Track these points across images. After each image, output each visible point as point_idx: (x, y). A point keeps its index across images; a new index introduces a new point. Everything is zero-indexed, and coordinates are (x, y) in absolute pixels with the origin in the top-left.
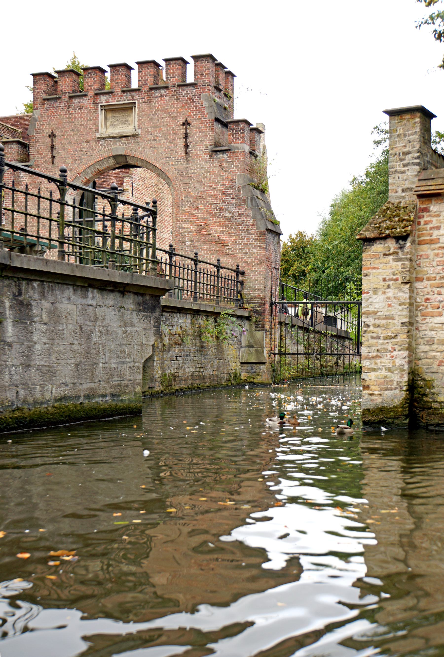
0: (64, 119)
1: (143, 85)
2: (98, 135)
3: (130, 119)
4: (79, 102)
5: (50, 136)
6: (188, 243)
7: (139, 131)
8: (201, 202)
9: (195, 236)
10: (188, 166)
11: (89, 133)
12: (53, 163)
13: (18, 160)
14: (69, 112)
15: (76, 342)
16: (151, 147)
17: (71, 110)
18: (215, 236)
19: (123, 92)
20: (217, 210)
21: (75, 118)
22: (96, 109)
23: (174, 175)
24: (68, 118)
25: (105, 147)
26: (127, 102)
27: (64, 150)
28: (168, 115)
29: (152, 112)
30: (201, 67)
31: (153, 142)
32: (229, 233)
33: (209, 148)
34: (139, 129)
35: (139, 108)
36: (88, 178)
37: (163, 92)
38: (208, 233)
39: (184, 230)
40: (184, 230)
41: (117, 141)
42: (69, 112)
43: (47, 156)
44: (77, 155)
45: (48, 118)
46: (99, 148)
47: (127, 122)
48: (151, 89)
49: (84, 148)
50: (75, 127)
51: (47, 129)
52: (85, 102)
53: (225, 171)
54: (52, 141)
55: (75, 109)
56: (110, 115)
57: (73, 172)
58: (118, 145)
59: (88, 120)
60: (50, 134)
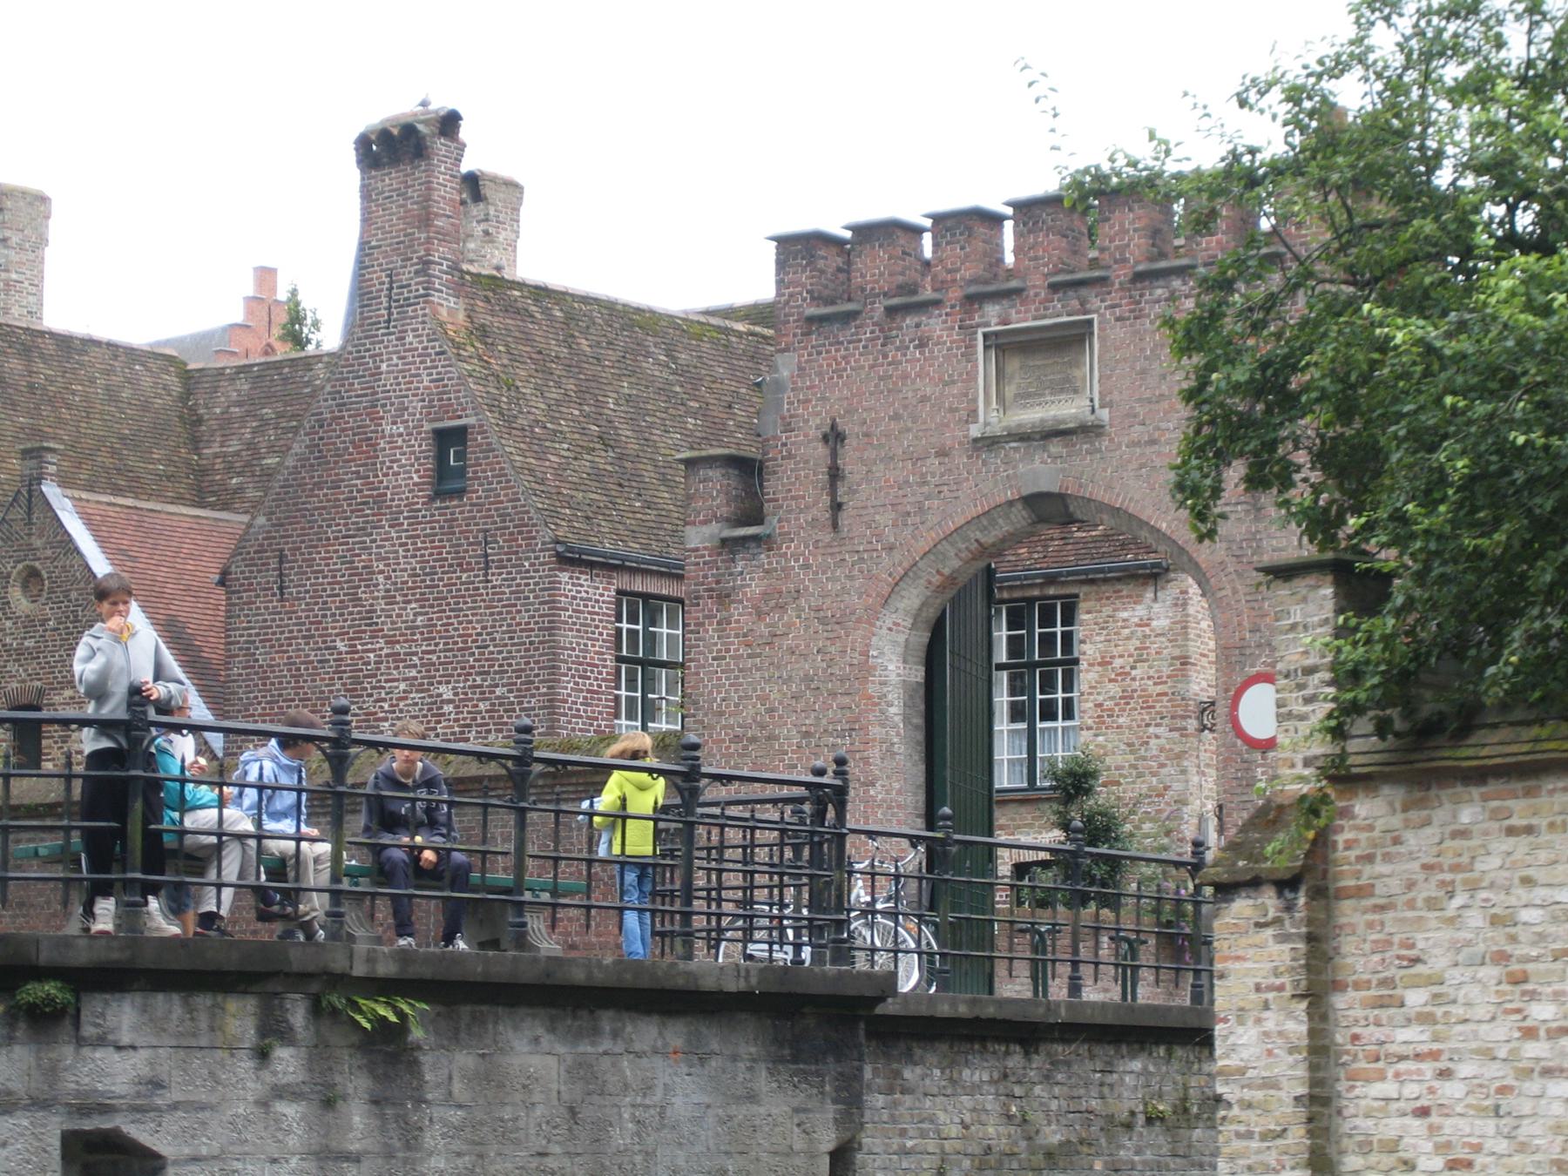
1: (1116, 262)
2: (975, 431)
3: (1077, 373)
4: (918, 326)
5: (825, 438)
7: (1104, 414)
10: (1261, 526)
11: (947, 425)
12: (835, 526)
13: (728, 520)
15: (557, 1149)
17: (891, 352)
19: (1055, 288)
21: (905, 377)
22: (971, 346)
24: (881, 379)
27: (869, 482)
29: (1142, 350)
31: (1148, 450)
34: (1102, 407)
35: (1102, 339)
36: (947, 571)
37: (1176, 283)
42: (885, 356)
43: (816, 503)
44: (911, 499)
45: (821, 380)
46: (979, 472)
47: (1069, 387)
48: (1139, 277)
50: (905, 407)
51: (819, 414)
52: (935, 325)
54: (834, 455)
55: (903, 348)
56: (1013, 364)
57: (897, 556)
58: (1037, 462)
59: (946, 384)
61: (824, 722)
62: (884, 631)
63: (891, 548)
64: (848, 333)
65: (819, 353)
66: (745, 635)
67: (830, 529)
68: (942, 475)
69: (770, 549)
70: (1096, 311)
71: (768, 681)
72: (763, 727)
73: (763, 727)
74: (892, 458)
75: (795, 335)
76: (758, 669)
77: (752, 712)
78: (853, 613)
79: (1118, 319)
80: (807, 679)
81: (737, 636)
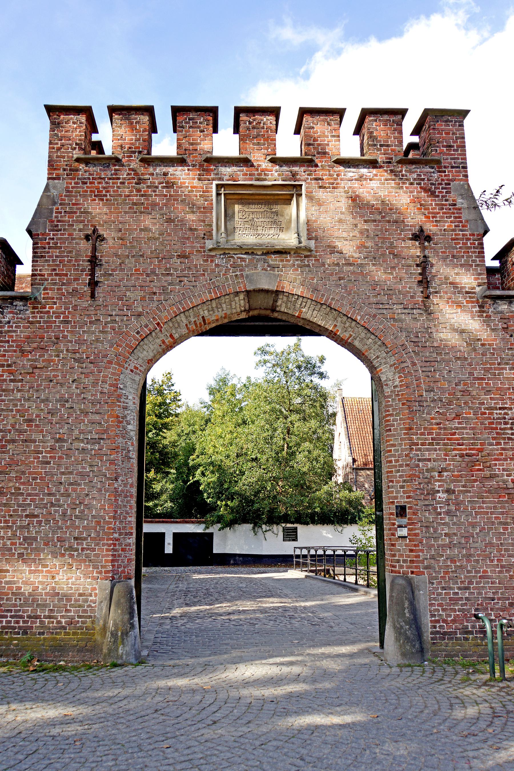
0: (127, 204)
1: (318, 153)
6: (442, 496)
9: (456, 479)
12: (93, 296)
14: (139, 191)
16: (340, 279)
17: (143, 186)
18: (505, 482)
20: (506, 423)
23: (399, 343)
25: (227, 270)
28: (379, 217)
30: (446, 134)
33: (478, 289)
37: (364, 171)
38: (487, 473)
39: (430, 465)
40: (430, 465)
41: (258, 260)
44: (159, 284)
46: (213, 271)
49: (176, 270)
54: (94, 249)
57: (144, 320)
60: (90, 232)
61: (77, 432)
62: (128, 371)
63: (139, 315)
64: (109, 173)
66: (9, 366)
67: (89, 298)
68: (184, 270)
69: (34, 308)
70: (305, 181)
73: (20, 432)
75: (64, 170)
76: (19, 391)
77: (12, 421)
78: (106, 356)
79: (320, 187)
80: (63, 401)
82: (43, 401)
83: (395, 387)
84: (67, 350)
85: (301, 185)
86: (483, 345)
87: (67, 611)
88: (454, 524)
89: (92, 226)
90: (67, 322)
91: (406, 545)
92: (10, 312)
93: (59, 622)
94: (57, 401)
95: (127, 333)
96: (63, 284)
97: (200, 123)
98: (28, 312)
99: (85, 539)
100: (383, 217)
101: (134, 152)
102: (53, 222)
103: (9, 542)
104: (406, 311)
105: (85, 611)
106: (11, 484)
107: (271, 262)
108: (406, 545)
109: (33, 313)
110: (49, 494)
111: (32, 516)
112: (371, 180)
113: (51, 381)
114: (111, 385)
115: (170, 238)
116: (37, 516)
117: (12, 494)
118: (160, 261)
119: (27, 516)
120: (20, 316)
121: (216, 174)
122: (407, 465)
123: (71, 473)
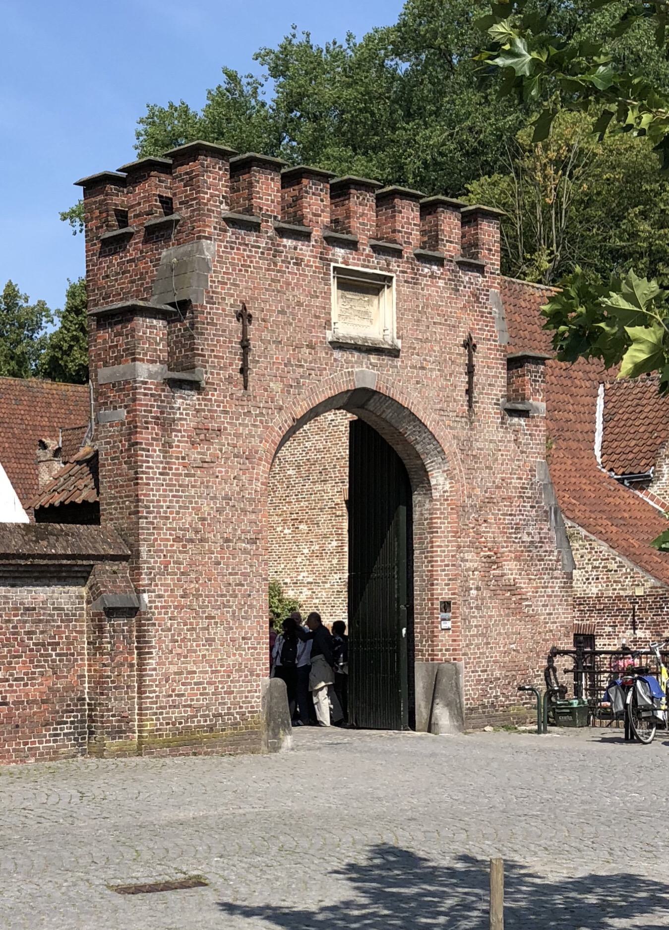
0: (267, 279)
1: (405, 242)
2: (329, 335)
3: (372, 309)
7: (399, 344)
8: (490, 510)
16: (418, 383)
18: (509, 579)
20: (512, 528)
23: (452, 450)
24: (273, 280)
26: (378, 272)
27: (266, 357)
32: (528, 575)
39: (468, 565)
42: (275, 264)
43: (231, 364)
44: (293, 377)
45: (234, 270)
46: (332, 365)
49: (306, 362)
51: (232, 295)
52: (305, 250)
53: (522, 452)
63: (281, 409)
65: (232, 248)
66: (183, 458)
70: (395, 272)
71: (200, 497)
72: (197, 532)
74: (280, 342)
75: (215, 228)
76: (193, 486)
77: (189, 519)
79: (406, 282)
80: (227, 498)
81: (177, 458)
82: (212, 498)
83: (444, 492)
84: (228, 444)
85: (392, 278)
86: (502, 455)
87: (241, 707)
88: (480, 617)
89: (241, 301)
90: (225, 412)
91: (449, 636)
92: (181, 397)
93: (235, 718)
94: (223, 499)
95: (272, 428)
96: (221, 368)
97: (321, 190)
98: (195, 398)
99: (250, 639)
100: (446, 320)
101: (270, 216)
102: (209, 292)
103: (195, 644)
104: (458, 419)
105: (252, 707)
106: (192, 585)
107: (372, 361)
108: (449, 636)
109: (198, 399)
110: (222, 596)
111: (210, 617)
112: (439, 278)
113: (217, 477)
114: (262, 484)
115: (299, 324)
116: (214, 618)
117: (193, 595)
118: (294, 350)
119: (207, 618)
120: (188, 402)
121: (333, 255)
122: (453, 565)
123: (236, 574)
